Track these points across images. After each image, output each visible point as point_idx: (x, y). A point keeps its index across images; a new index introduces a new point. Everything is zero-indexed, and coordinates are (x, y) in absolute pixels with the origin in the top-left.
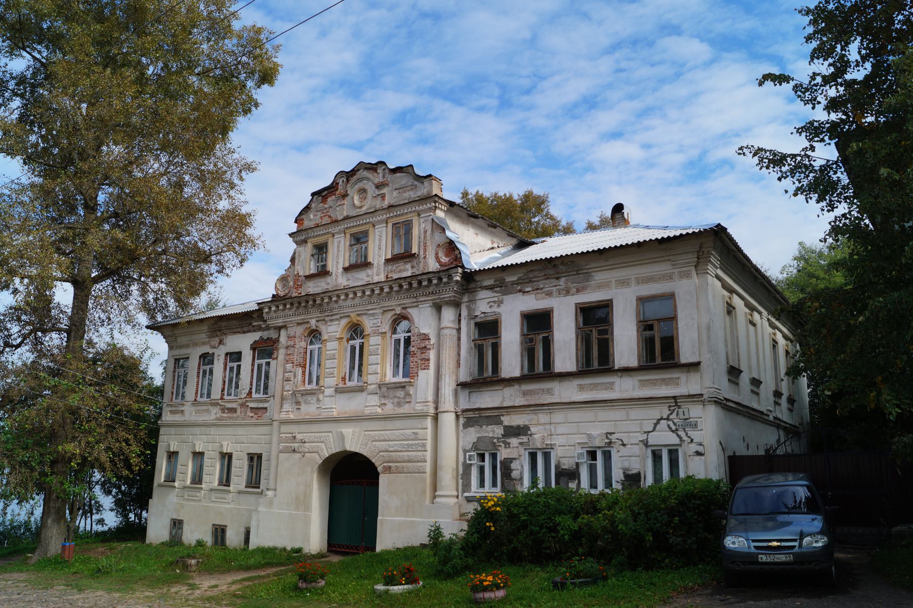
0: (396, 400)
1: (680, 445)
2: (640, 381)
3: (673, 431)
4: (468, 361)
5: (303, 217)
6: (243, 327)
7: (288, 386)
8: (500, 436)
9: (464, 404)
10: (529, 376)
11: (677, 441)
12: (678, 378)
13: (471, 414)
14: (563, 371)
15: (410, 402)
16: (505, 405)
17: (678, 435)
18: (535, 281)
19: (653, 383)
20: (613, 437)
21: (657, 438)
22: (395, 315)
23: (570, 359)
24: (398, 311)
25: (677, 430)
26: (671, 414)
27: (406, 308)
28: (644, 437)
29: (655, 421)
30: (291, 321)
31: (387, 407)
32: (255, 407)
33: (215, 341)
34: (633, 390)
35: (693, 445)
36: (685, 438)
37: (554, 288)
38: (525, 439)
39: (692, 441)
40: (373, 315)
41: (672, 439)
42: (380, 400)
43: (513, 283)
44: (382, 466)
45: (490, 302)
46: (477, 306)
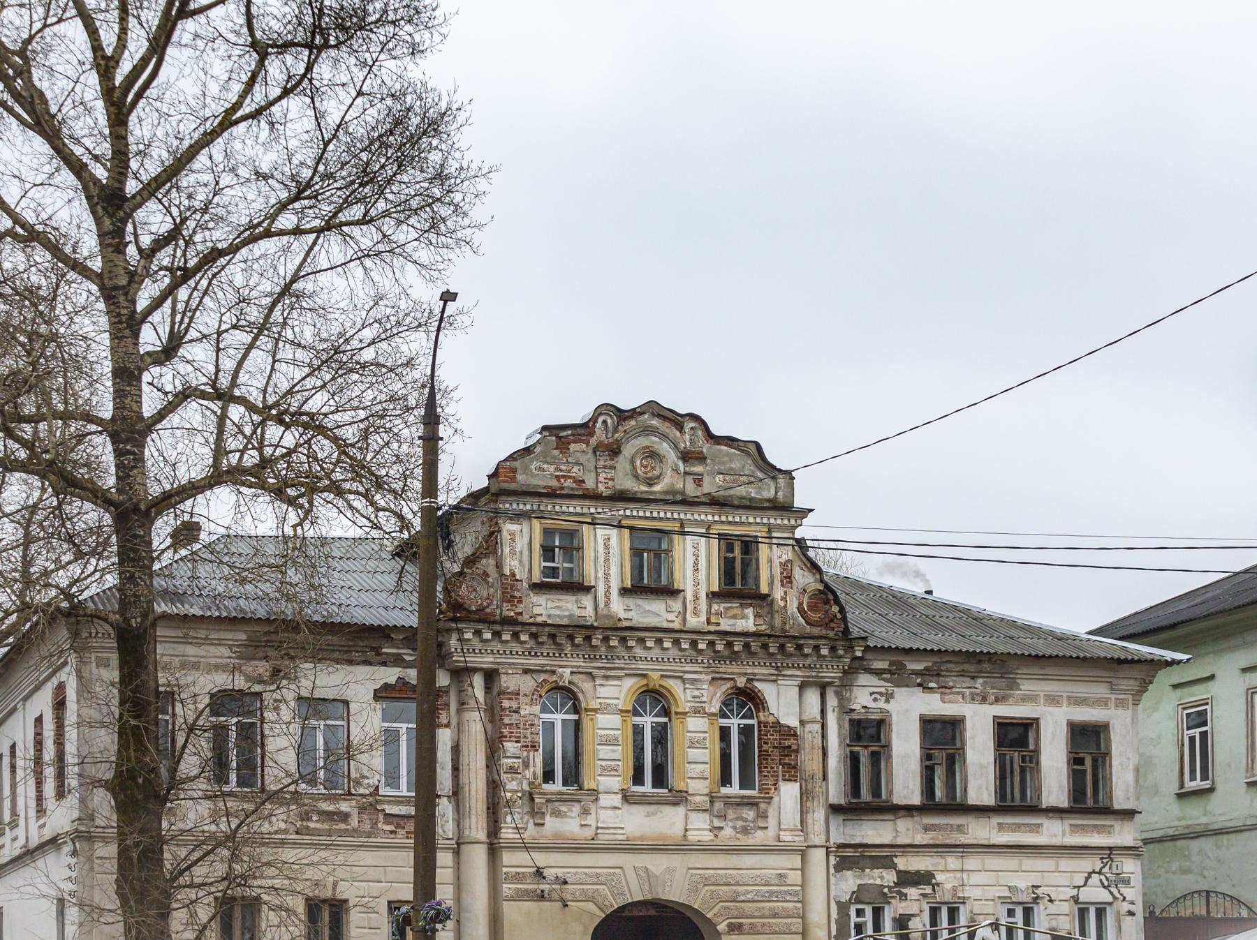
0: (740, 823)
1: (1110, 904)
2: (1071, 825)
3: (1104, 887)
4: (840, 773)
5: (517, 464)
6: (350, 651)
7: (515, 783)
8: (892, 884)
9: (837, 838)
10: (929, 806)
11: (1110, 899)
12: (1112, 826)
13: (849, 852)
14: (978, 803)
15: (766, 828)
16: (900, 841)
17: (1110, 891)
18: (943, 676)
19: (1083, 829)
20: (1039, 891)
21: (1088, 894)
22: (732, 688)
23: (987, 789)
24: (741, 682)
25: (1109, 886)
26: (1104, 867)
27: (752, 680)
28: (1075, 892)
29: (1086, 875)
30: (513, 664)
31: (723, 832)
32: (403, 813)
33: (263, 668)
34: (1064, 835)
35: (1125, 904)
36: (1117, 895)
37: (968, 691)
38: (928, 890)
39: (1124, 898)
40: (693, 681)
41: (1104, 896)
42: (712, 821)
43: (917, 673)
44: (726, 923)
45: (874, 693)
46: (853, 695)
